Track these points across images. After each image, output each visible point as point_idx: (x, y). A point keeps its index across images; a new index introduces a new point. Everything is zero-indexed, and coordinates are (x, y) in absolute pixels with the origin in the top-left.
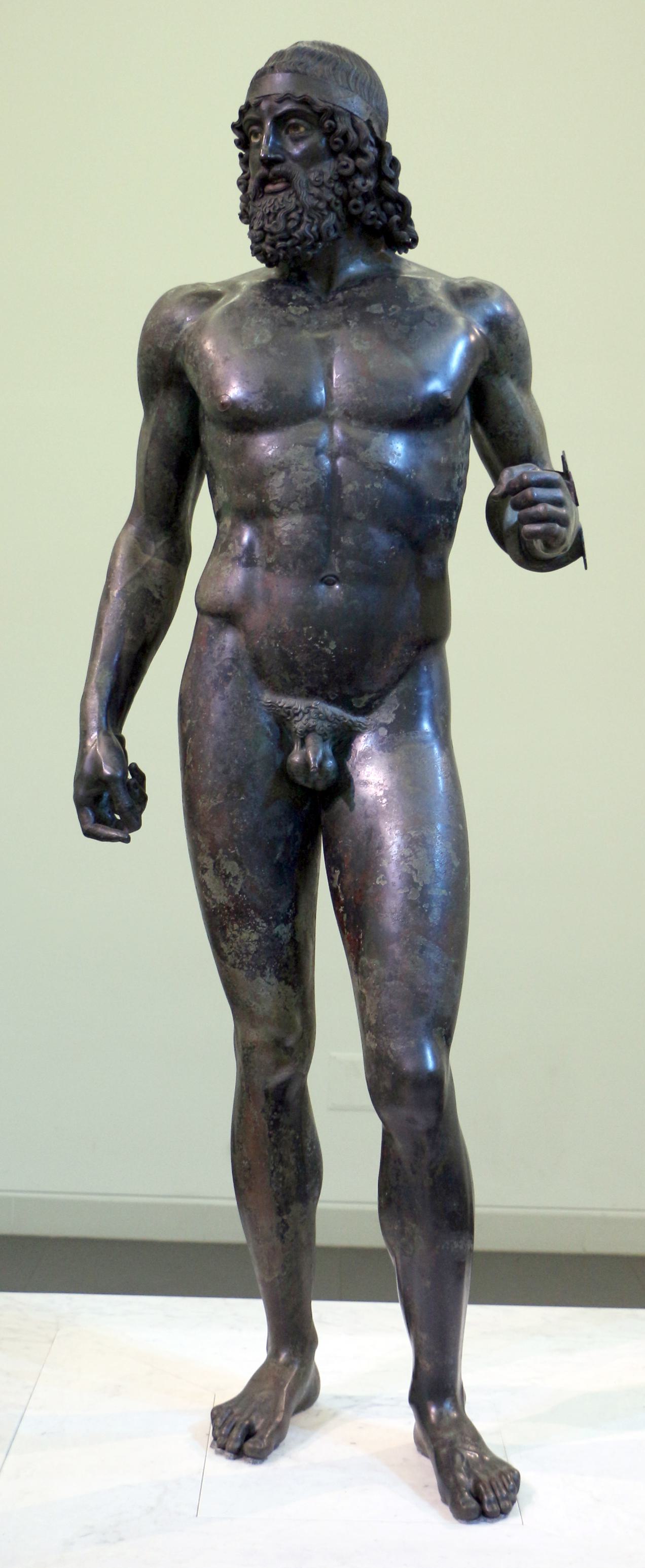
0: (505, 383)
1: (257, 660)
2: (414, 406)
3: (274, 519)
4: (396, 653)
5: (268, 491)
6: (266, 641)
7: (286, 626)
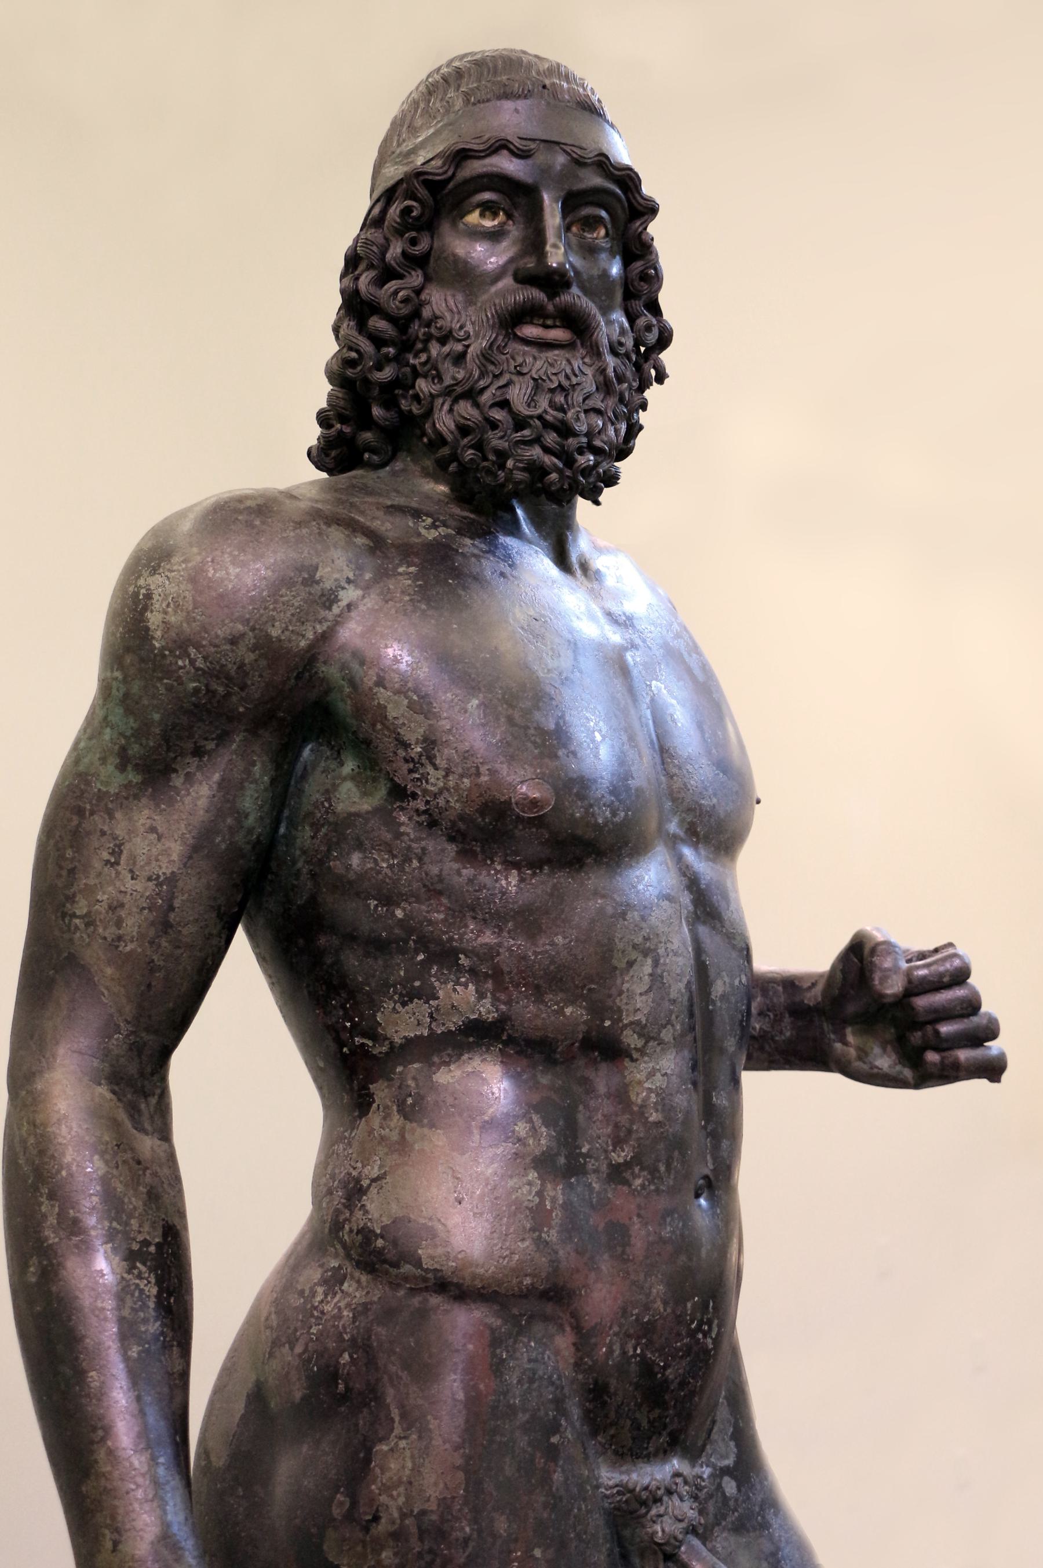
1: (597, 1393)
3: (627, 1062)
5: (621, 1002)
6: (617, 1348)
7: (659, 1305)
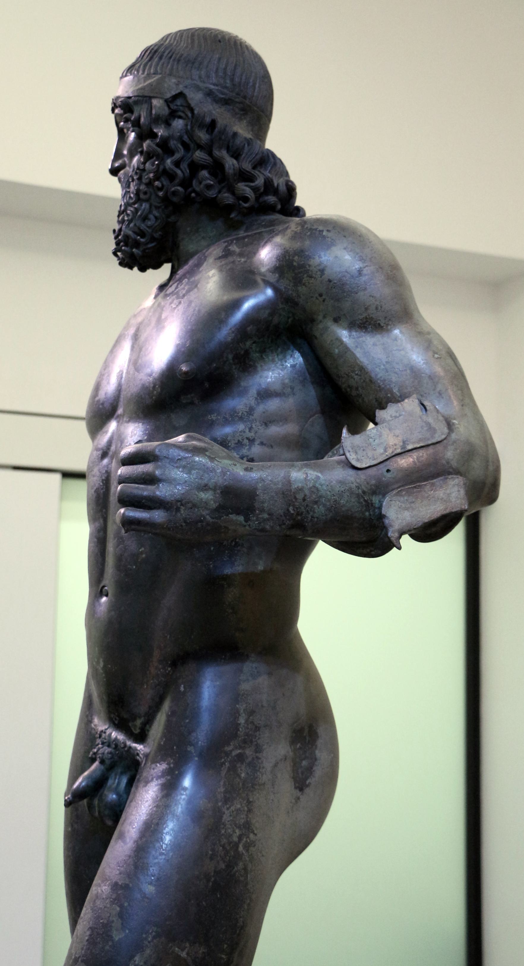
0: (326, 329)
2: (154, 387)
4: (153, 670)
